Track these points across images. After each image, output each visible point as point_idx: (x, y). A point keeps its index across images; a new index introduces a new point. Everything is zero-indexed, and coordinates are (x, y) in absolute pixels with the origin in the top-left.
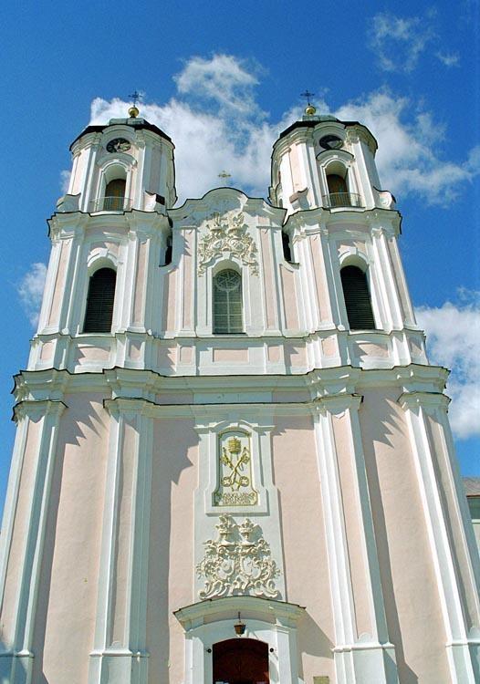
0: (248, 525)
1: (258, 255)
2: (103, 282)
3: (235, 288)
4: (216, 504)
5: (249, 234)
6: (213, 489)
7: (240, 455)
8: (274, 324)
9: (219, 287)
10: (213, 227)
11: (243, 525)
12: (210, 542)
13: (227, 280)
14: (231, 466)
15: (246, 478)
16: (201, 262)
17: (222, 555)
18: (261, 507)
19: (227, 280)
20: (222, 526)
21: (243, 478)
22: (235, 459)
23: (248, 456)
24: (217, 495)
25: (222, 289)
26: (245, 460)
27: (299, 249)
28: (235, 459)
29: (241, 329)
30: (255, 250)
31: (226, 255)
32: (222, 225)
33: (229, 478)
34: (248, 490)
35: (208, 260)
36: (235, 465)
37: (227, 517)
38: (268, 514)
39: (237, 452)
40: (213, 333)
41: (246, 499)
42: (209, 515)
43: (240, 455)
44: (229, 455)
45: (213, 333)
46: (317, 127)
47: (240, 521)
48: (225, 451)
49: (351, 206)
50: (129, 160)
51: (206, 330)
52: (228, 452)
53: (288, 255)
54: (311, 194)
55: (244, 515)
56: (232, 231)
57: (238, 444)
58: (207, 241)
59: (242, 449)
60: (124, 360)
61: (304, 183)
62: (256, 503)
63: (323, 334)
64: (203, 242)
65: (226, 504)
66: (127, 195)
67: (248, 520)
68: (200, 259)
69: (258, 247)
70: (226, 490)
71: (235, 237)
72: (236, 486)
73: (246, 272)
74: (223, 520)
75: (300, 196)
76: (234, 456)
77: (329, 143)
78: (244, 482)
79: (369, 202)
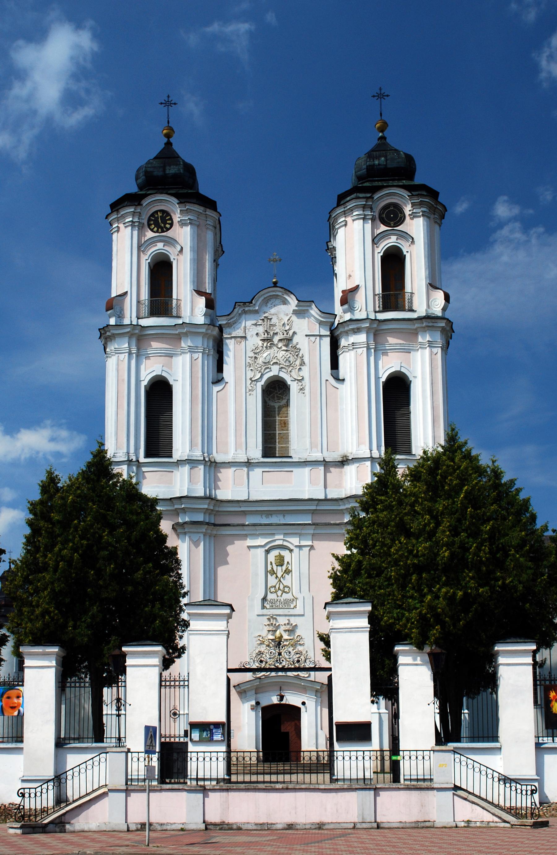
0: (288, 624)
1: (305, 369)
2: (159, 394)
4: (263, 607)
5: (297, 343)
6: (262, 597)
7: (284, 568)
8: (316, 447)
9: (267, 399)
10: (263, 336)
11: (285, 624)
12: (260, 636)
13: (276, 392)
14: (277, 577)
15: (288, 587)
16: (251, 379)
17: (268, 646)
18: (299, 610)
19: (276, 392)
20: (268, 625)
21: (285, 587)
22: (280, 571)
23: (290, 568)
24: (264, 599)
25: (272, 404)
26: (288, 572)
28: (280, 571)
29: (287, 449)
30: (303, 363)
31: (275, 371)
32: (272, 333)
33: (275, 587)
34: (288, 596)
35: (259, 375)
36: (279, 576)
37: (272, 618)
38: (303, 615)
39: (282, 565)
40: (264, 456)
41: (287, 603)
42: (258, 615)
43: (284, 568)
44: (275, 568)
45: (264, 456)
47: (282, 621)
48: (271, 563)
49: (404, 310)
50: (171, 242)
51: (256, 452)
52: (274, 565)
53: (335, 364)
54: (362, 291)
55: (286, 615)
56: (280, 340)
57: (280, 561)
58: (256, 353)
59: (286, 563)
60: (187, 487)
62: (295, 607)
64: (252, 355)
65: (272, 607)
66: (174, 296)
67: (289, 620)
68: (250, 374)
69: (306, 360)
70: (270, 596)
71: (284, 348)
72: (279, 593)
73: (294, 387)
74: (269, 619)
75: (348, 298)
76: (279, 568)
77: (392, 217)
78: (286, 589)
79: (420, 309)
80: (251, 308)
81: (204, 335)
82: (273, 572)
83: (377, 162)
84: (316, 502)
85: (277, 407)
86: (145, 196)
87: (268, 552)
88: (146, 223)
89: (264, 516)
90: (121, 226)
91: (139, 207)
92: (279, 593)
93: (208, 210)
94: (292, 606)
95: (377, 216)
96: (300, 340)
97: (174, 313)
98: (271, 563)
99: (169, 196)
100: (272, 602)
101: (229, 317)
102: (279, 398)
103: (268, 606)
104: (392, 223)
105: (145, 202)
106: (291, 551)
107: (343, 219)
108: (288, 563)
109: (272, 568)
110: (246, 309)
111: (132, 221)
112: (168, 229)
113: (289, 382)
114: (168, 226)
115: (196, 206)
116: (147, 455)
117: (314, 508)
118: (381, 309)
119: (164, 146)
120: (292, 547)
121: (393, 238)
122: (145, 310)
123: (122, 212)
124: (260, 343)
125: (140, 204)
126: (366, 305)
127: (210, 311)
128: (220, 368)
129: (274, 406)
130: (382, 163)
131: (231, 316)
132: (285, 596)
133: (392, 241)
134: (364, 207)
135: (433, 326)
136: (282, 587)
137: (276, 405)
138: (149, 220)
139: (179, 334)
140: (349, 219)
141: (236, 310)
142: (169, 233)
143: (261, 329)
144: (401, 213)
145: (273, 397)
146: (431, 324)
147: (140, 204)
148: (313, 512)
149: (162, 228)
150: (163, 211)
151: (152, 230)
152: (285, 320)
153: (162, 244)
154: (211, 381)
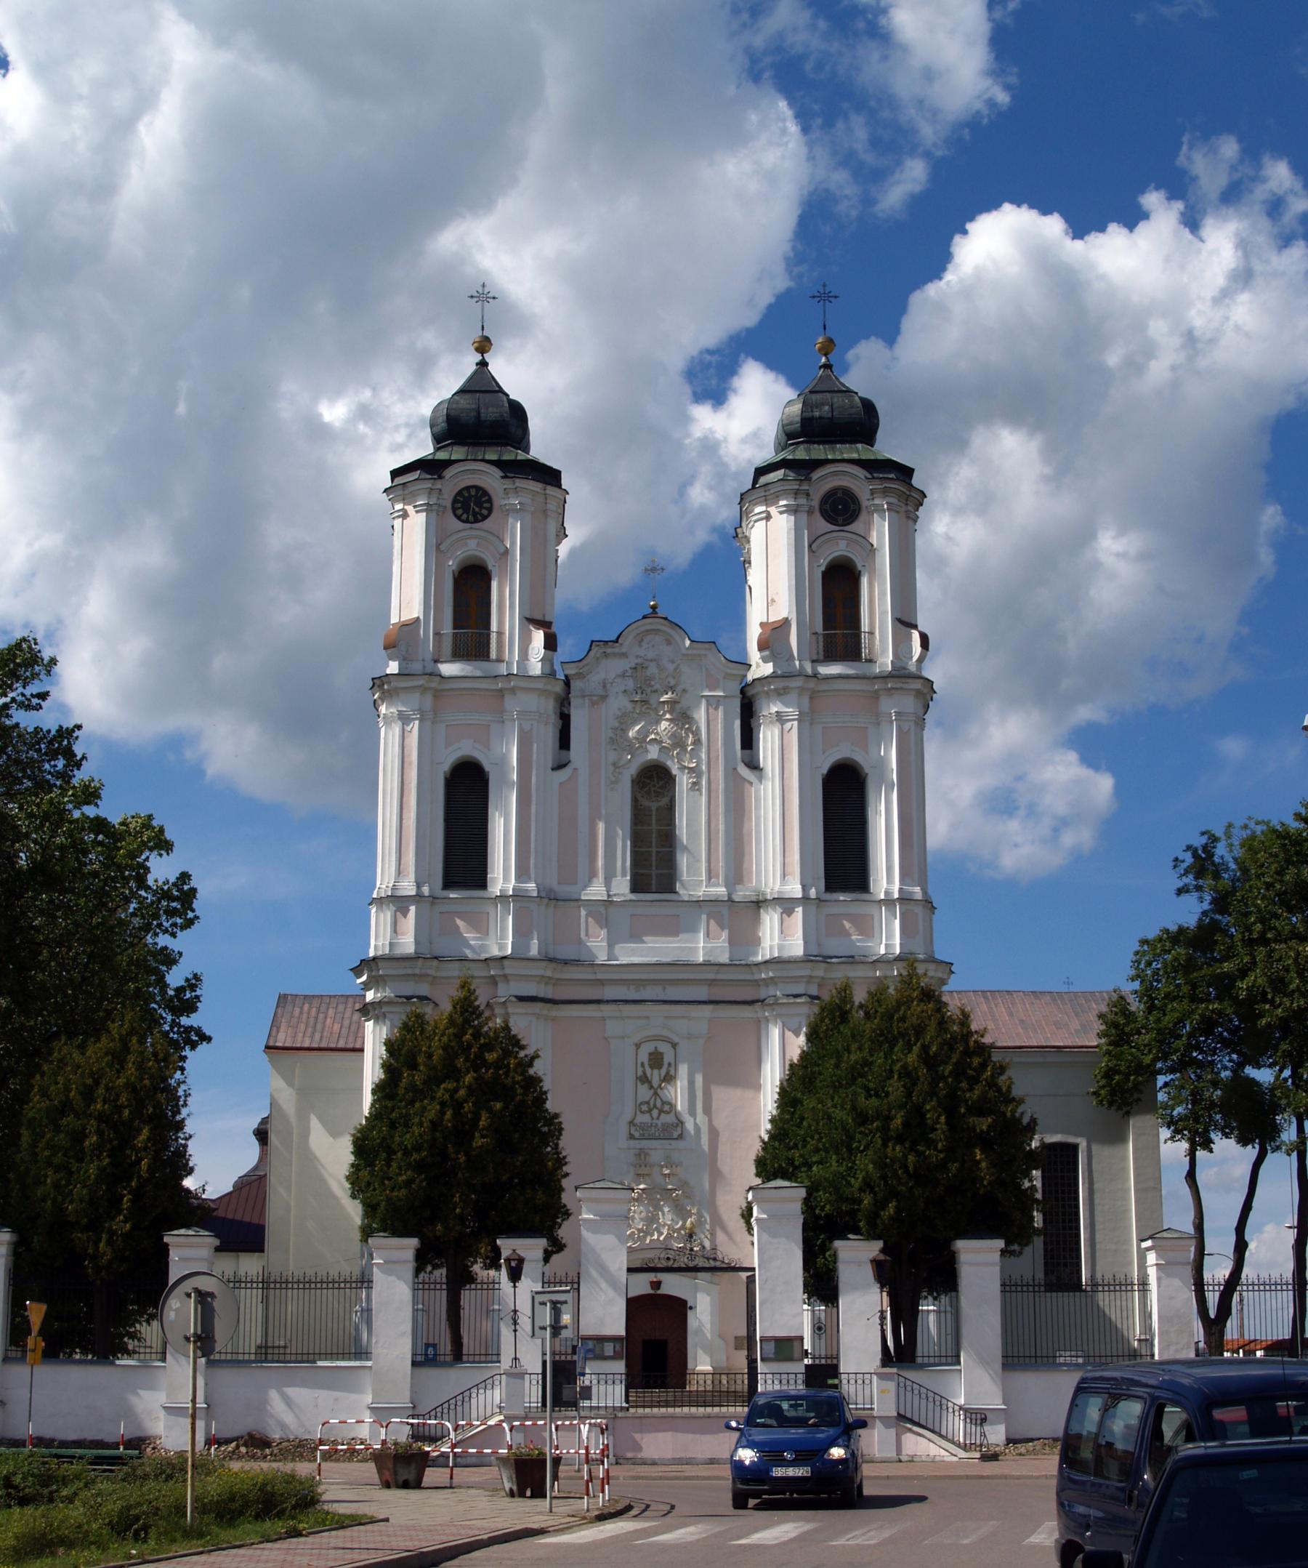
3: (664, 801)
7: (663, 1071)
8: (717, 877)
9: (639, 796)
14: (651, 1087)
22: (655, 1076)
23: (672, 1072)
27: (768, 738)
28: (655, 1076)
30: (697, 742)
31: (653, 754)
33: (648, 1103)
36: (655, 1084)
44: (648, 1071)
46: (816, 475)
48: (643, 1065)
61: (784, 608)
63: (786, 905)
66: (494, 627)
68: (612, 756)
72: (655, 1113)
73: (683, 782)
76: (656, 1071)
80: (616, 650)
81: (543, 692)
82: (644, 1079)
83: (817, 414)
84: (716, 968)
85: (654, 808)
87: (638, 1046)
88: (449, 506)
89: (632, 987)
90: (410, 509)
91: (439, 482)
92: (655, 1113)
93: (549, 487)
94: (675, 1135)
95: (817, 506)
97: (493, 655)
98: (643, 1065)
99: (488, 465)
100: (643, 1127)
101: (581, 664)
102: (658, 794)
103: (637, 1135)
104: (840, 519)
105: (449, 473)
106: (674, 1045)
107: (763, 508)
108: (670, 1064)
109: (644, 1073)
110: (609, 651)
111: (427, 504)
112: (485, 518)
113: (675, 771)
114: (485, 512)
115: (532, 483)
117: (711, 976)
118: (821, 657)
119: (474, 367)
120: (676, 1040)
121: (843, 544)
122: (447, 645)
124: (629, 706)
125: (440, 477)
127: (550, 653)
128: (564, 741)
129: (649, 809)
130: (825, 415)
131: (584, 662)
132: (665, 1119)
133: (839, 547)
134: (796, 493)
135: (901, 689)
136: (659, 1104)
137: (654, 806)
138: (455, 501)
139: (501, 690)
140: (773, 510)
141: (592, 653)
143: (630, 684)
144: (854, 503)
145: (649, 792)
146: (899, 685)
147: (440, 477)
148: (711, 983)
149: (475, 514)
150: (478, 488)
151: (459, 518)
152: (671, 667)
153: (475, 541)
154: (550, 766)
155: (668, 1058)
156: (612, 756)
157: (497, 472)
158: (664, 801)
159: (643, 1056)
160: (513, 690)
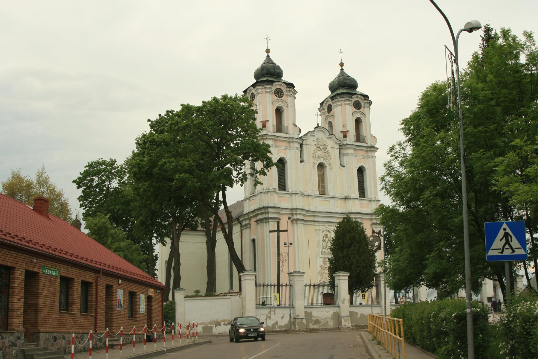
30: (331, 158)
31: (322, 160)
69: (332, 157)
73: (328, 167)
82: (324, 241)
86: (275, 82)
96: (329, 148)
100: (324, 252)
105: (274, 84)
106: (330, 232)
116: (279, 190)
123: (265, 86)
125: (272, 85)
126: (351, 138)
133: (359, 115)
138: (275, 91)
142: (282, 98)
147: (272, 85)
155: (329, 235)
156: (313, 161)
157: (285, 86)
158: (322, 172)
159: (324, 235)
160: (293, 142)
